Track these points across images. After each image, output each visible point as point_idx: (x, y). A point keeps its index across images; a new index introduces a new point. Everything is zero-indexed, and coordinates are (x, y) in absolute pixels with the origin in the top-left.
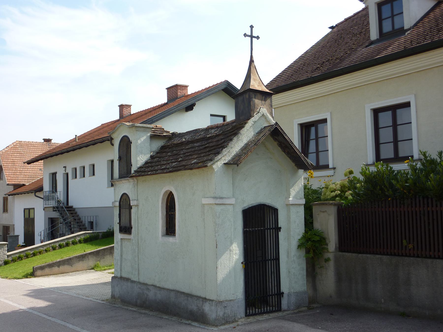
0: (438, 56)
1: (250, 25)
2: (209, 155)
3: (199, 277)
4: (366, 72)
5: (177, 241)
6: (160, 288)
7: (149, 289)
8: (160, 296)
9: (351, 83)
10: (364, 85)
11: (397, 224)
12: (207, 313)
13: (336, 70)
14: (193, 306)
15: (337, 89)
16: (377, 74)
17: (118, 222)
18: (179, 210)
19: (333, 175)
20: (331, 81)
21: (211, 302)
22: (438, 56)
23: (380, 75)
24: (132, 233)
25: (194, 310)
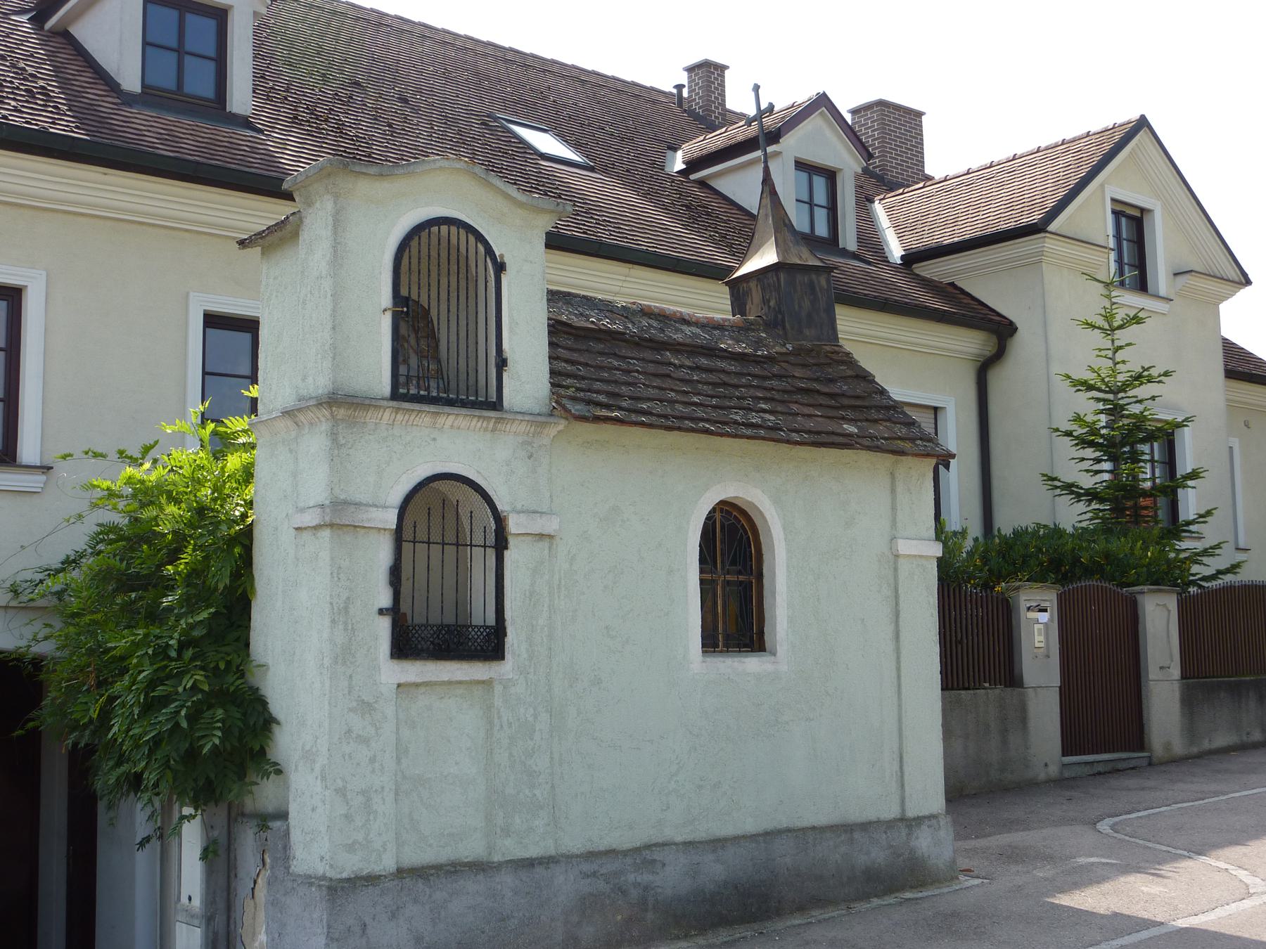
0: (928, 334)
1: (752, 87)
2: (876, 421)
3: (873, 765)
4: (240, 201)
5: (784, 668)
6: (717, 844)
7: (654, 861)
8: (715, 870)
9: (205, 217)
10: (187, 230)
11: (1186, 608)
12: (926, 855)
13: (254, 173)
14: (875, 854)
15: (89, 205)
16: (170, 206)
17: (385, 600)
18: (788, 567)
19: (39, 490)
20: (105, 174)
21: (934, 822)
22: (928, 334)
23: (721, 305)
24: (508, 655)
25: (880, 864)
